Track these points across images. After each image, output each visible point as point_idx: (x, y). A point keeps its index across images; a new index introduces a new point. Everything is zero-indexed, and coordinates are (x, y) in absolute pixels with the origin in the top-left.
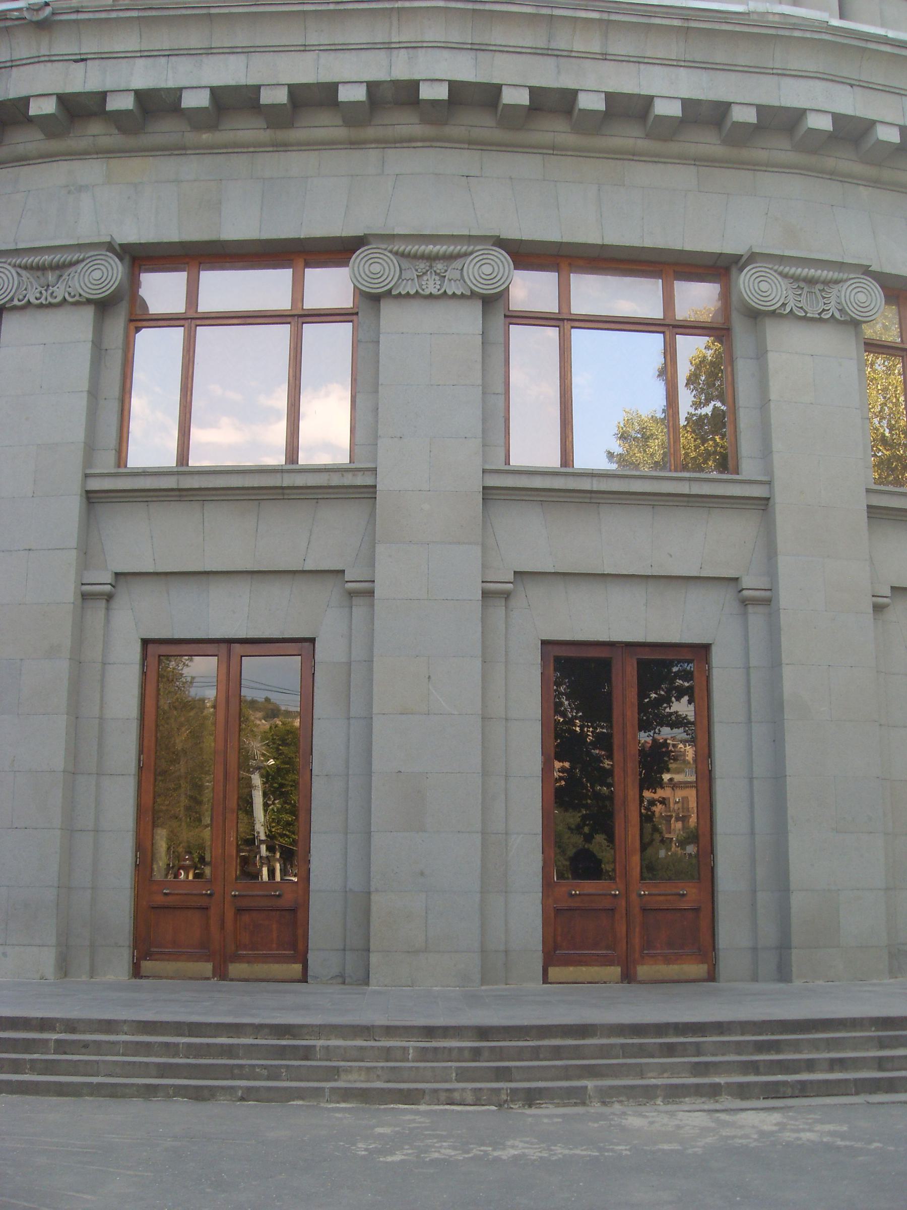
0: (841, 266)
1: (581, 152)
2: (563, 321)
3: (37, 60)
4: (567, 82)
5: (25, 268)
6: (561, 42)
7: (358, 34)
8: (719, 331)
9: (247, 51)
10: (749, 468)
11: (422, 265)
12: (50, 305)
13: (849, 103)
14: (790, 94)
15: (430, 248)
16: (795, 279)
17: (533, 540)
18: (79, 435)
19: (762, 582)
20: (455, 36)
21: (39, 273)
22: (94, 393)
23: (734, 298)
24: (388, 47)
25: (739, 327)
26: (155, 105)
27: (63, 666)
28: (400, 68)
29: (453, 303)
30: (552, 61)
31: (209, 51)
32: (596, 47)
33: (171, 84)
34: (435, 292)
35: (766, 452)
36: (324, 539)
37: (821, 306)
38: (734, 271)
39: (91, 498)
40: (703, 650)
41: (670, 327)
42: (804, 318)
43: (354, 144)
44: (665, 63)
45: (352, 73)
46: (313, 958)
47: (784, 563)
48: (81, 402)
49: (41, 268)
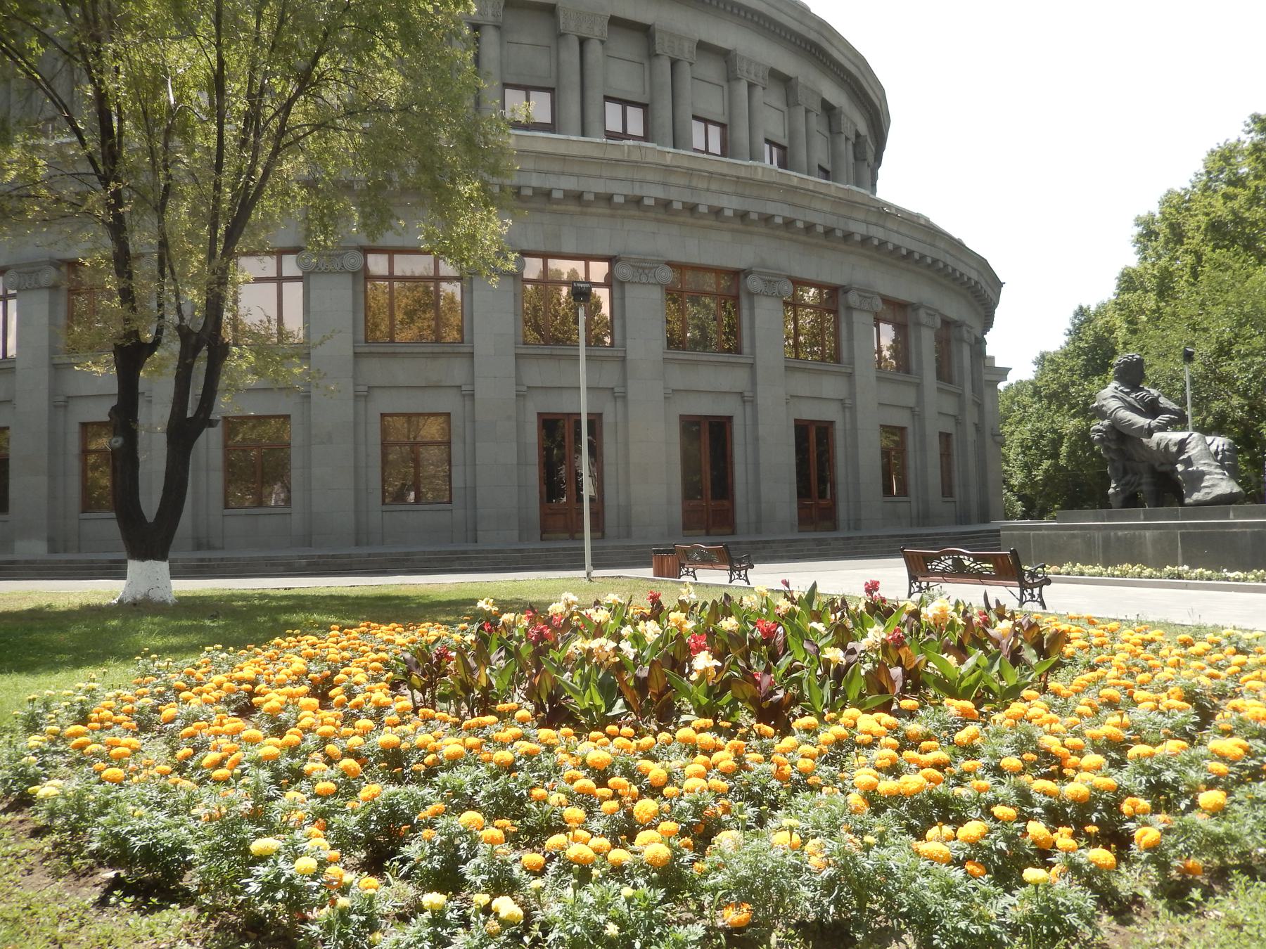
4: (694, 200)
6: (694, 184)
10: (746, 349)
14: (770, 209)
31: (563, 174)
35: (753, 346)
38: (742, 276)
40: (730, 418)
43: (613, 216)
47: (759, 388)
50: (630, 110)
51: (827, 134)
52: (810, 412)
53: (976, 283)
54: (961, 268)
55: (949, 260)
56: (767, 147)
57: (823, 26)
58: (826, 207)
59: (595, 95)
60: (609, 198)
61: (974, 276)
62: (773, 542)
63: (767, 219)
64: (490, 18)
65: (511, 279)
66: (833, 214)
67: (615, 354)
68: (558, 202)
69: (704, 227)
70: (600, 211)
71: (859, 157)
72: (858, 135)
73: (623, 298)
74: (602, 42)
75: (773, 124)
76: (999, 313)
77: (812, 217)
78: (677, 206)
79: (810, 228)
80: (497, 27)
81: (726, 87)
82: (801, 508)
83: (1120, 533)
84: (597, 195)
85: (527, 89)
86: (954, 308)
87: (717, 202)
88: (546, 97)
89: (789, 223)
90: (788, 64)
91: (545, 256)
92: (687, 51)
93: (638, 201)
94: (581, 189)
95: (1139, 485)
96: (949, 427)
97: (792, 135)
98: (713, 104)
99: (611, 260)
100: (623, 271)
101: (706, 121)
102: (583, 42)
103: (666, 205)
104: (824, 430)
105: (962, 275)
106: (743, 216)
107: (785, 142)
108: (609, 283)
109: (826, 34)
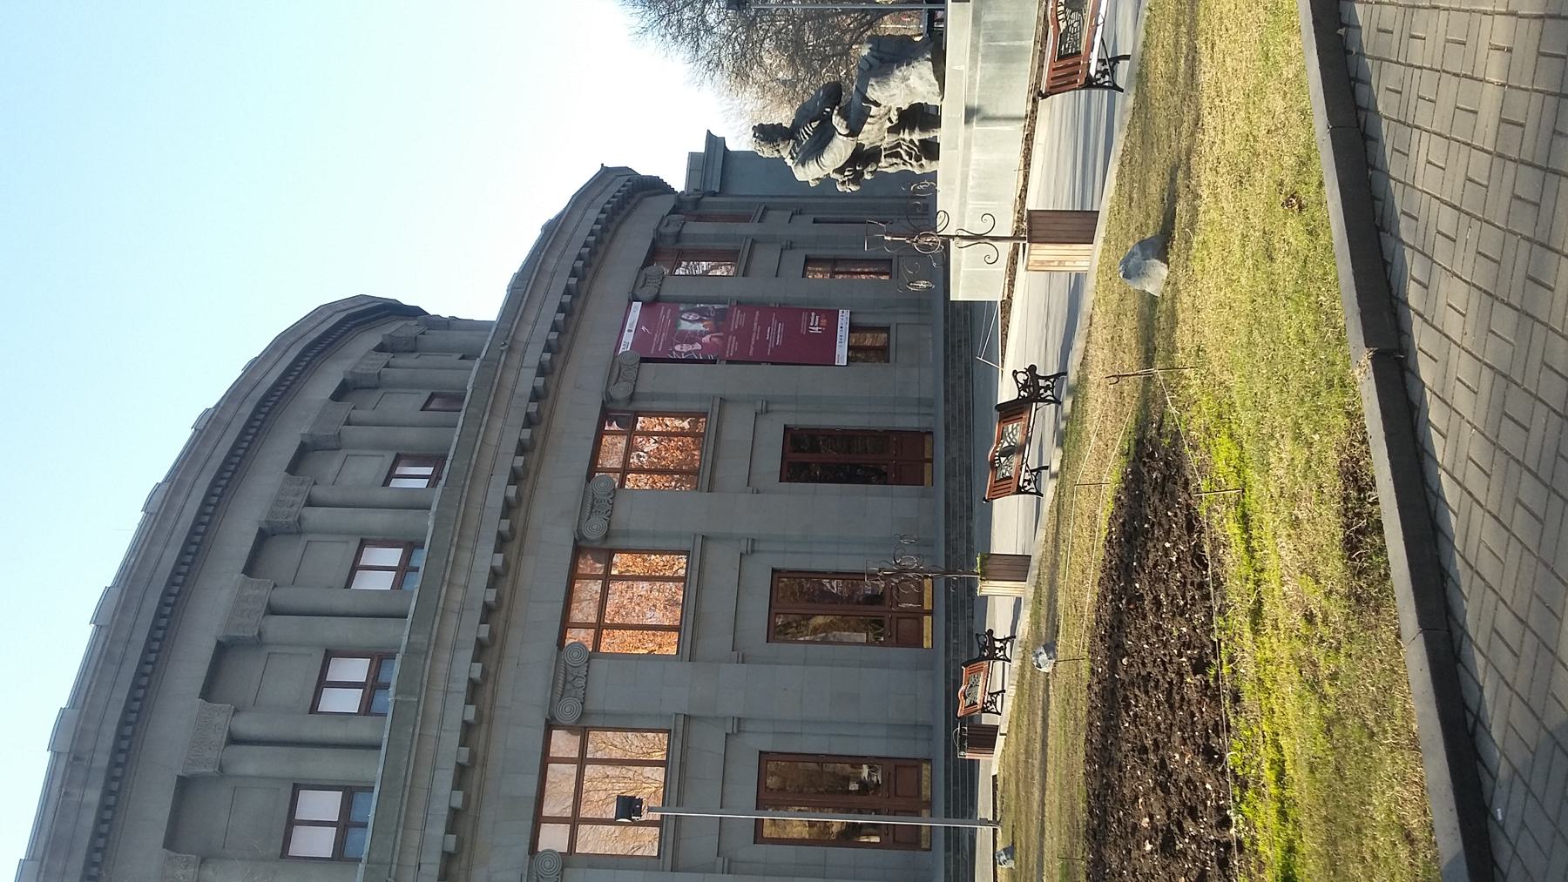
1: (509, 609)
2: (599, 627)
4: (478, 607)
6: (456, 606)
7: (436, 708)
8: (608, 556)
11: (568, 686)
14: (495, 501)
17: (716, 640)
19: (744, 542)
20: (446, 656)
23: (596, 544)
25: (610, 544)
31: (430, 790)
36: (709, 741)
38: (582, 543)
43: (490, 723)
45: (459, 711)
46: (920, 755)
50: (332, 676)
51: (380, 392)
53: (602, 212)
54: (583, 234)
55: (573, 251)
56: (395, 483)
57: (235, 394)
59: (312, 729)
60: (467, 727)
61: (593, 214)
62: (947, 535)
63: (508, 508)
65: (567, 871)
67: (680, 729)
68: (467, 798)
69: (513, 594)
70: (482, 741)
71: (411, 347)
72: (381, 348)
73: (605, 714)
74: (236, 711)
75: (365, 470)
76: (644, 170)
78: (484, 631)
79: (522, 449)
81: (310, 537)
82: (900, 481)
83: (971, 183)
84: (463, 744)
85: (291, 822)
86: (634, 241)
88: (305, 797)
89: (515, 477)
90: (282, 447)
91: (538, 819)
92: (259, 591)
93: (474, 687)
94: (453, 766)
95: (912, 141)
96: (798, 257)
97: (381, 446)
98: (336, 555)
99: (550, 726)
100: (568, 710)
101: (355, 567)
102: (234, 740)
103: (481, 648)
104: (796, 440)
105: (592, 233)
106: (502, 542)
107: (390, 457)
108: (582, 731)
109: (246, 389)
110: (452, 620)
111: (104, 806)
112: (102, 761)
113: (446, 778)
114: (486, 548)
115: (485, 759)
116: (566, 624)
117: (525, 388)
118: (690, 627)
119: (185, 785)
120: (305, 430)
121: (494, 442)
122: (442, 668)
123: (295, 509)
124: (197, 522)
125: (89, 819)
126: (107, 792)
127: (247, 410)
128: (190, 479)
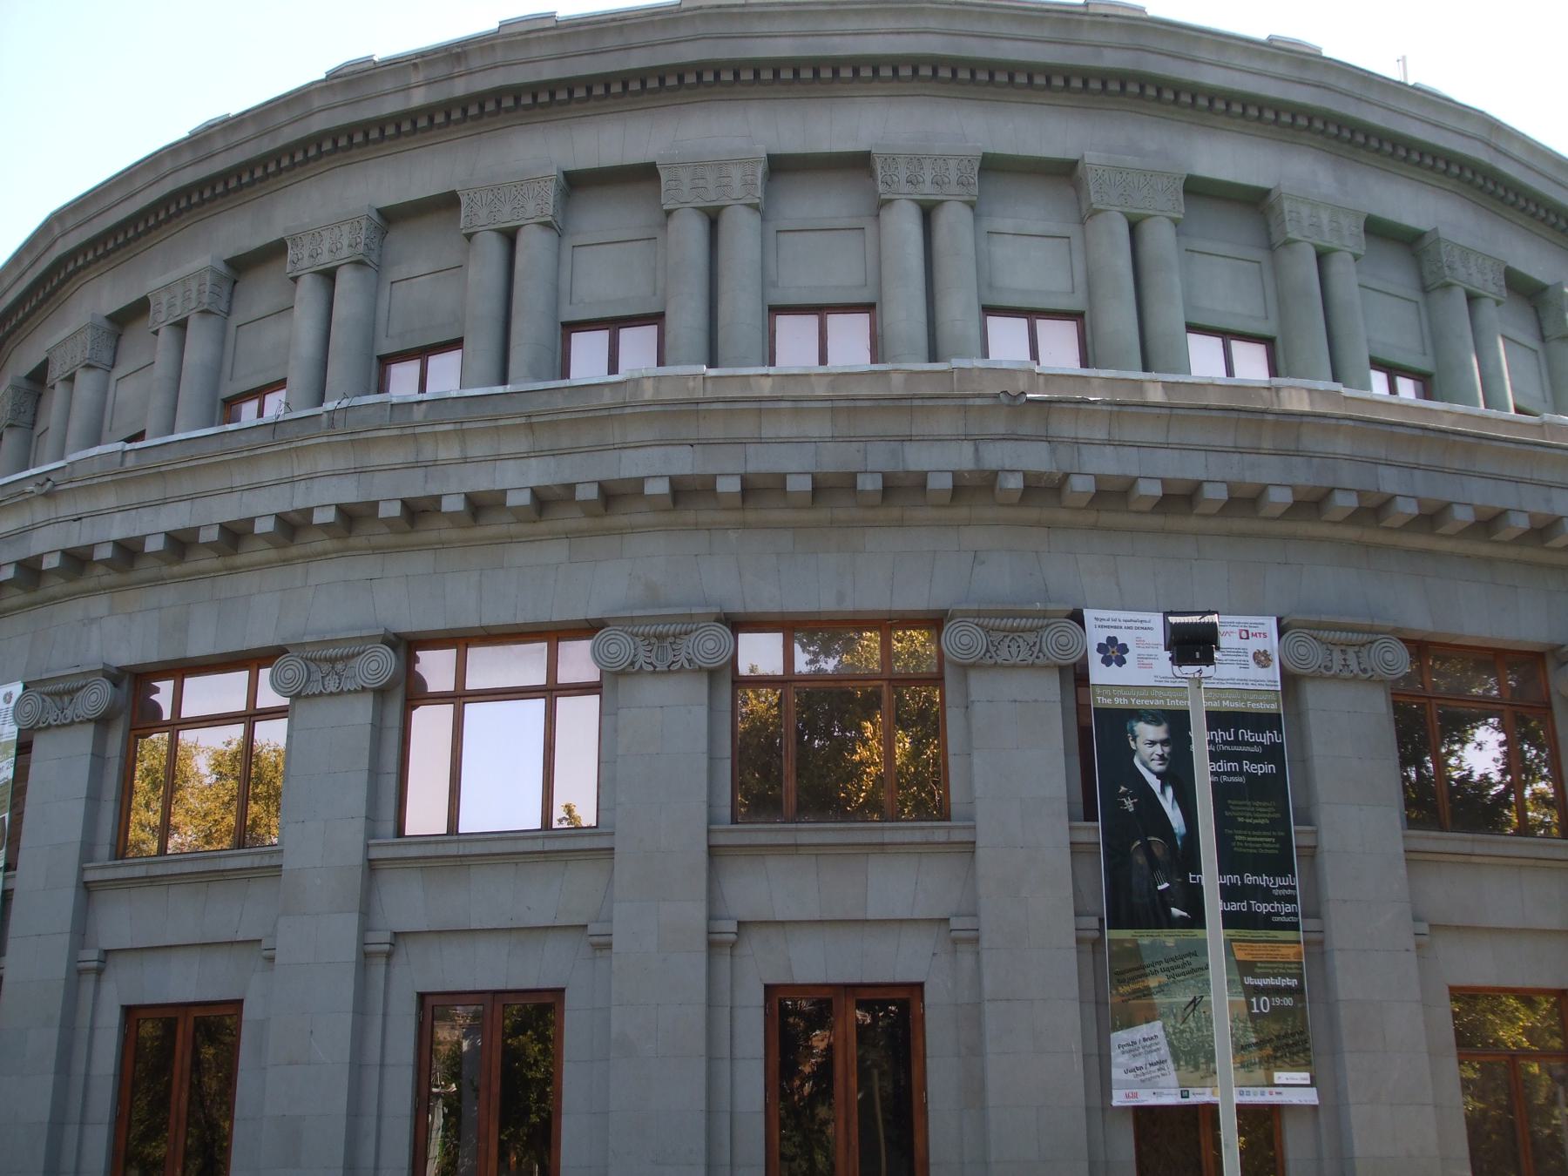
0: (691, 617)
3: (48, 523)
4: (433, 489)
5: (48, 694)
6: (428, 453)
7: (268, 473)
9: (192, 498)
11: (326, 667)
12: (64, 725)
13: (684, 463)
14: (629, 466)
15: (331, 652)
16: (646, 637)
18: (76, 835)
20: (341, 464)
21: (57, 699)
22: (94, 797)
24: (292, 481)
26: (128, 551)
27: (54, 1033)
28: (298, 499)
29: (350, 697)
30: (420, 472)
31: (164, 502)
32: (455, 453)
33: (137, 533)
34: (334, 690)
37: (671, 658)
39: (87, 889)
41: (551, 691)
42: (654, 672)
43: (287, 562)
44: (516, 457)
48: (79, 809)
49: (60, 694)
52: (815, 963)
58: (817, 428)
64: (346, 252)
66: (849, 440)
77: (762, 461)
80: (359, 264)
81: (870, 231)
87: (481, 481)
102: (510, 237)
107: (1075, 303)
110: (400, 455)
111: (412, 115)
112: (460, 88)
113: (177, 518)
114: (541, 473)
115: (233, 570)
116: (460, 640)
117: (918, 458)
118: (461, 854)
119: (448, 202)
120: (1092, 157)
121: (768, 432)
122: (324, 463)
123: (907, 188)
124: (856, 63)
125: (391, 106)
126: (429, 111)
127: (1112, 60)
128: (933, 24)
